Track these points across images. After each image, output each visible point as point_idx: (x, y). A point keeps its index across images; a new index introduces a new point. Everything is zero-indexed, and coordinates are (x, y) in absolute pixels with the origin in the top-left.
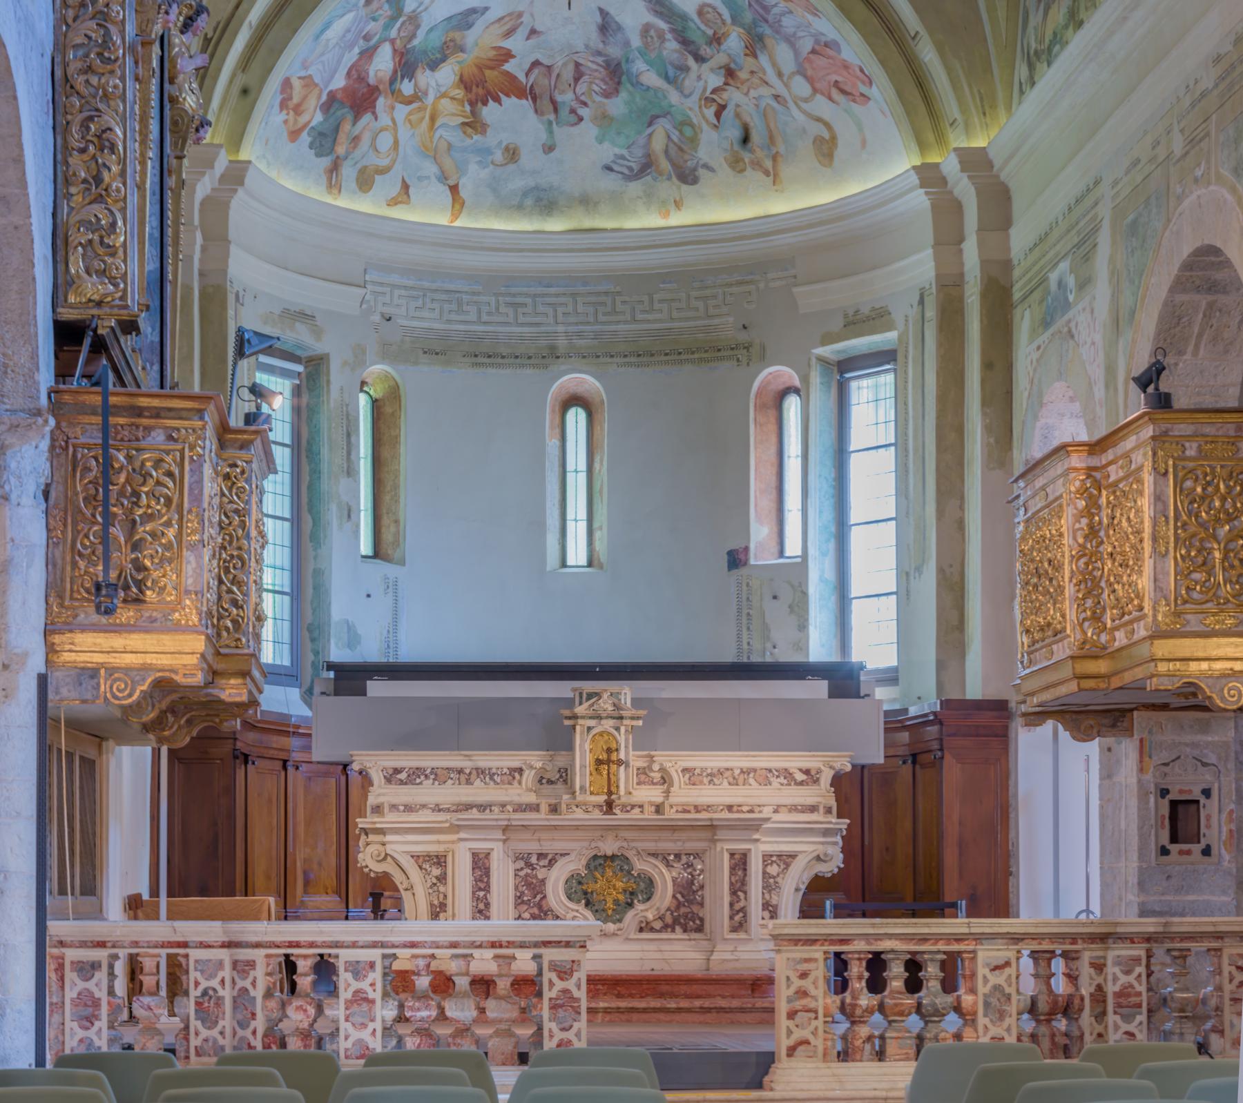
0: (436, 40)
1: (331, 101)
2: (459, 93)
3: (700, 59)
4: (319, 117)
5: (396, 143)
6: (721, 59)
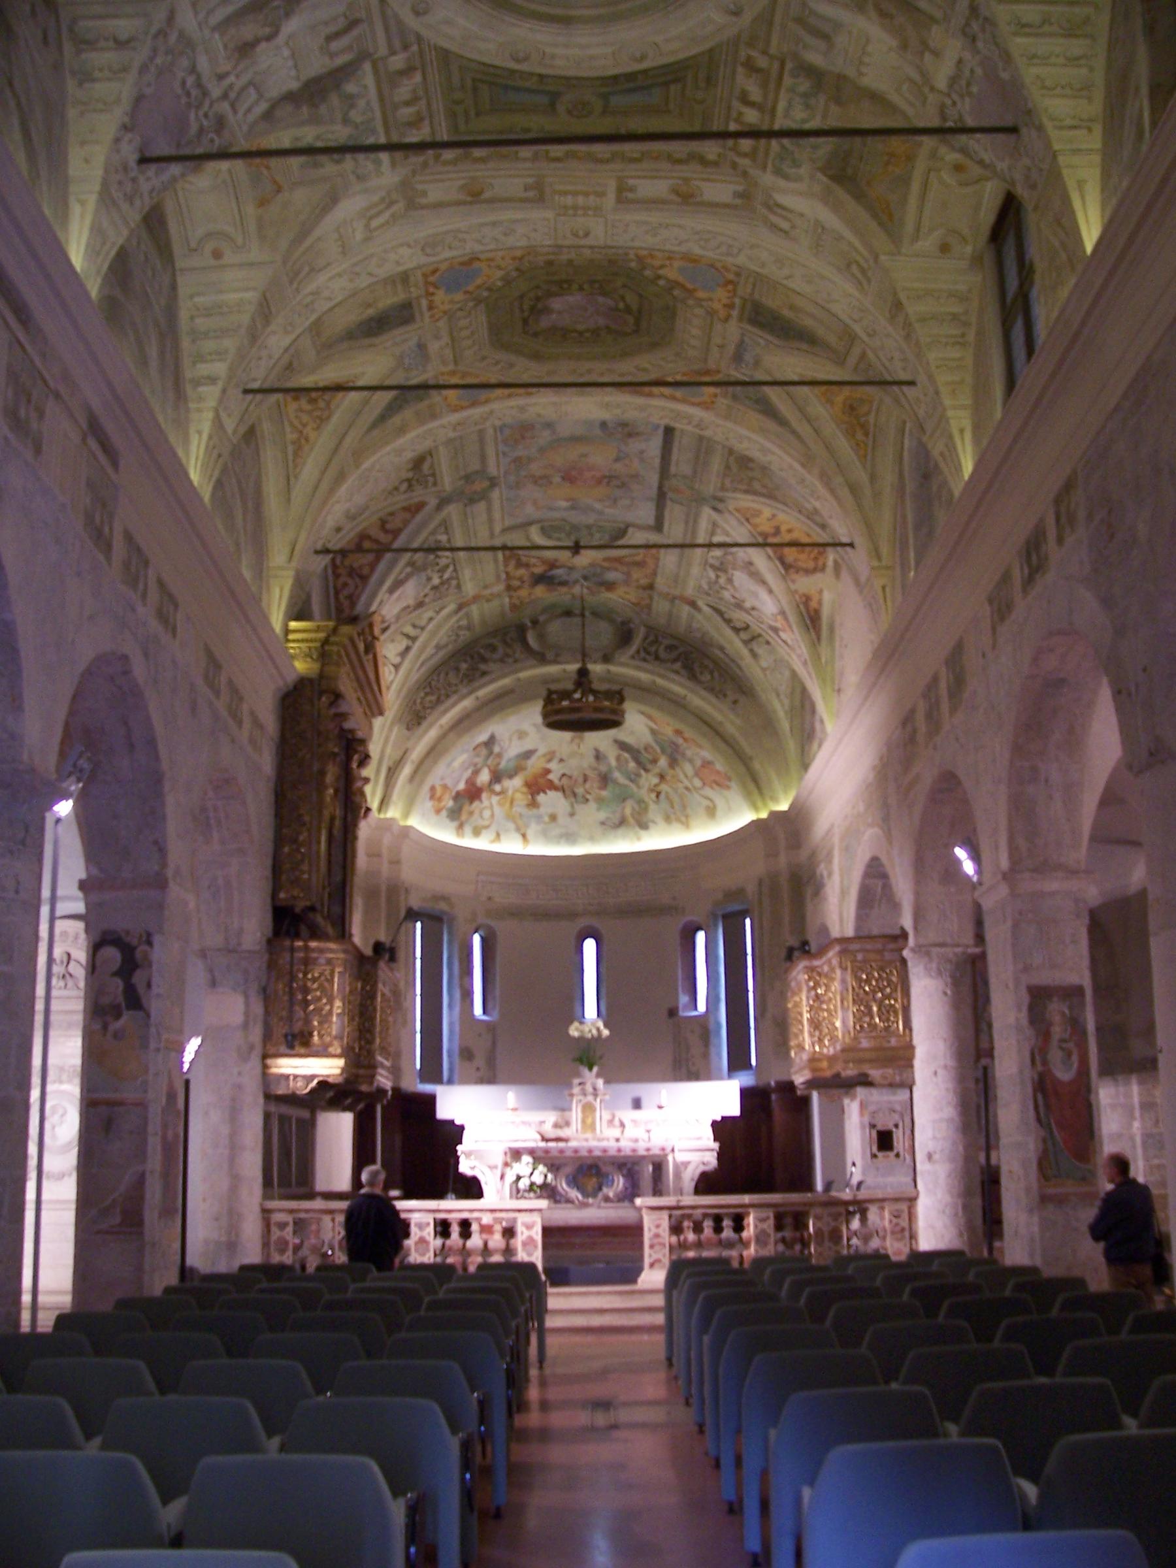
0: (512, 765)
1: (458, 796)
2: (525, 790)
3: (647, 770)
4: (451, 803)
5: (492, 815)
6: (657, 770)
